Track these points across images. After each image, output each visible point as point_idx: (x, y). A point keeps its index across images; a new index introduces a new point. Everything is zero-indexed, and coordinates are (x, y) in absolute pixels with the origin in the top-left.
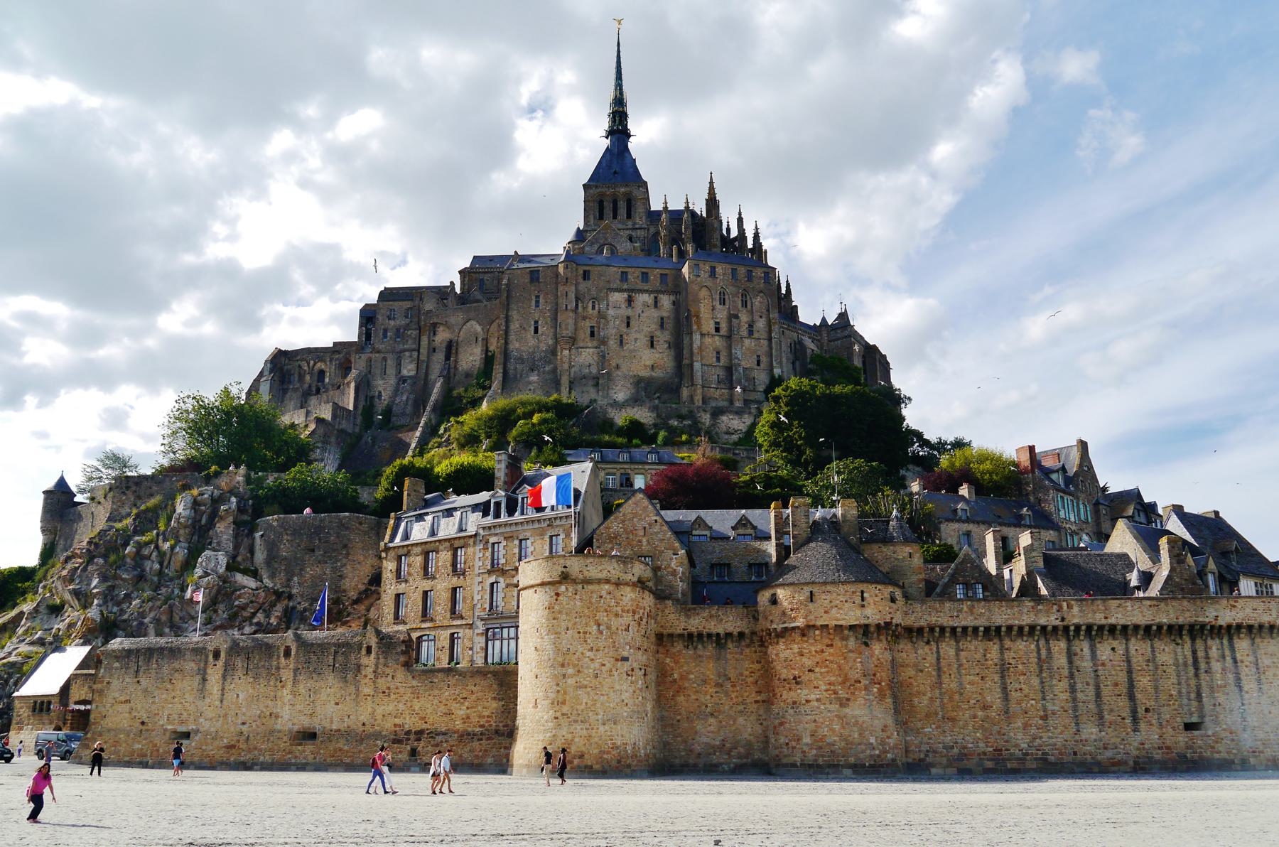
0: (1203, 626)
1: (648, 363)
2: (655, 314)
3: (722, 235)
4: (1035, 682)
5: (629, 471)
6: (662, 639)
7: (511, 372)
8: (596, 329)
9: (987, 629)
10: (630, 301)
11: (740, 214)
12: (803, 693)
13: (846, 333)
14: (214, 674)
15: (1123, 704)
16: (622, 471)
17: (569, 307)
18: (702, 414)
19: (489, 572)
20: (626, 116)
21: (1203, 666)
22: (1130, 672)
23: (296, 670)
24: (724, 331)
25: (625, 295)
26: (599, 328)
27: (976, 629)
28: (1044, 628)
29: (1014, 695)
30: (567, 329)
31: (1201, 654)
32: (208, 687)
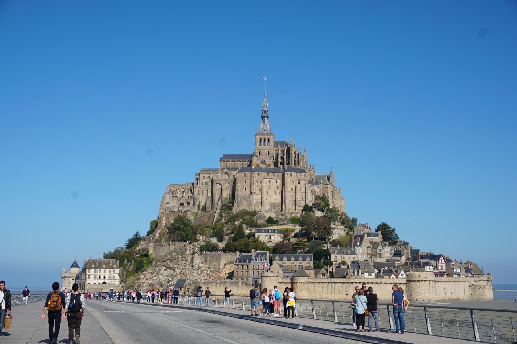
0: (349, 282)
1: (274, 198)
2: (276, 185)
4: (327, 289)
7: (239, 200)
8: (261, 189)
9: (321, 282)
10: (270, 181)
12: (296, 290)
14: (218, 286)
15: (338, 292)
17: (254, 184)
18: (287, 214)
19: (252, 270)
21: (349, 287)
22: (339, 288)
23: (230, 286)
24: (294, 190)
25: (268, 180)
28: (328, 282)
29: (324, 290)
31: (349, 286)
32: (217, 288)
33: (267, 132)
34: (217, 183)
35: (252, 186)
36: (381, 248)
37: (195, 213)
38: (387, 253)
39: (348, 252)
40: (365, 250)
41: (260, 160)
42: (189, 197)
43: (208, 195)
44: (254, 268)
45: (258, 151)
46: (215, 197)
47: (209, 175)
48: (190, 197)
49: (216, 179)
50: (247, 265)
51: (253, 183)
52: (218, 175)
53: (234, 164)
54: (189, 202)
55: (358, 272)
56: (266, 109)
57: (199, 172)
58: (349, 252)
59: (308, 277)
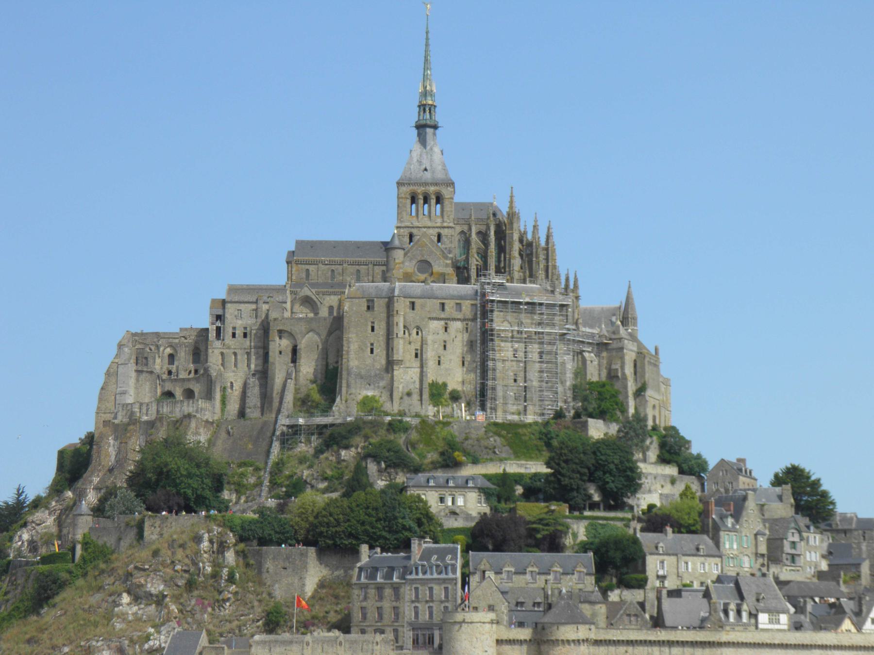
3: (520, 231)
5: (454, 493)
6: (499, 642)
8: (419, 352)
9: (628, 641)
11: (536, 221)
13: (620, 345)
16: (450, 493)
17: (399, 336)
19: (413, 602)
20: (435, 106)
23: (345, 651)
25: (442, 323)
26: (422, 350)
27: (623, 641)
30: (398, 353)
33: (433, 172)
34: (281, 332)
35: (393, 342)
36: (796, 538)
37: (212, 423)
38: (813, 554)
39: (698, 549)
40: (748, 542)
41: (414, 262)
42: (190, 372)
43: (253, 366)
44: (417, 596)
45: (406, 232)
46: (274, 374)
47: (254, 306)
48: (193, 372)
49: (275, 319)
50: (395, 586)
51: (395, 332)
52: (284, 305)
53: (333, 271)
54: (191, 387)
55: (739, 612)
56: (430, 102)
57: (223, 296)
58: (701, 547)
59: (587, 626)
